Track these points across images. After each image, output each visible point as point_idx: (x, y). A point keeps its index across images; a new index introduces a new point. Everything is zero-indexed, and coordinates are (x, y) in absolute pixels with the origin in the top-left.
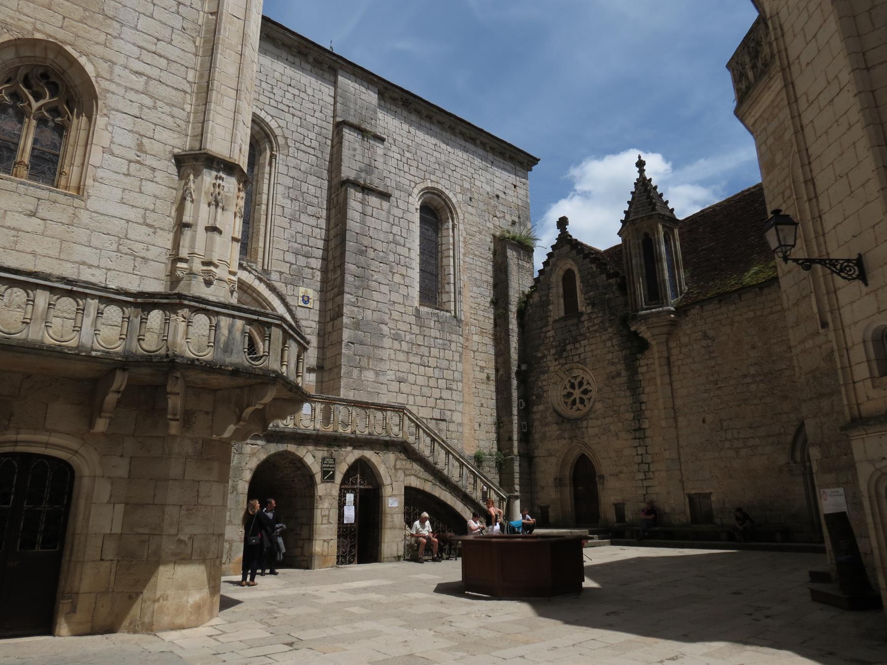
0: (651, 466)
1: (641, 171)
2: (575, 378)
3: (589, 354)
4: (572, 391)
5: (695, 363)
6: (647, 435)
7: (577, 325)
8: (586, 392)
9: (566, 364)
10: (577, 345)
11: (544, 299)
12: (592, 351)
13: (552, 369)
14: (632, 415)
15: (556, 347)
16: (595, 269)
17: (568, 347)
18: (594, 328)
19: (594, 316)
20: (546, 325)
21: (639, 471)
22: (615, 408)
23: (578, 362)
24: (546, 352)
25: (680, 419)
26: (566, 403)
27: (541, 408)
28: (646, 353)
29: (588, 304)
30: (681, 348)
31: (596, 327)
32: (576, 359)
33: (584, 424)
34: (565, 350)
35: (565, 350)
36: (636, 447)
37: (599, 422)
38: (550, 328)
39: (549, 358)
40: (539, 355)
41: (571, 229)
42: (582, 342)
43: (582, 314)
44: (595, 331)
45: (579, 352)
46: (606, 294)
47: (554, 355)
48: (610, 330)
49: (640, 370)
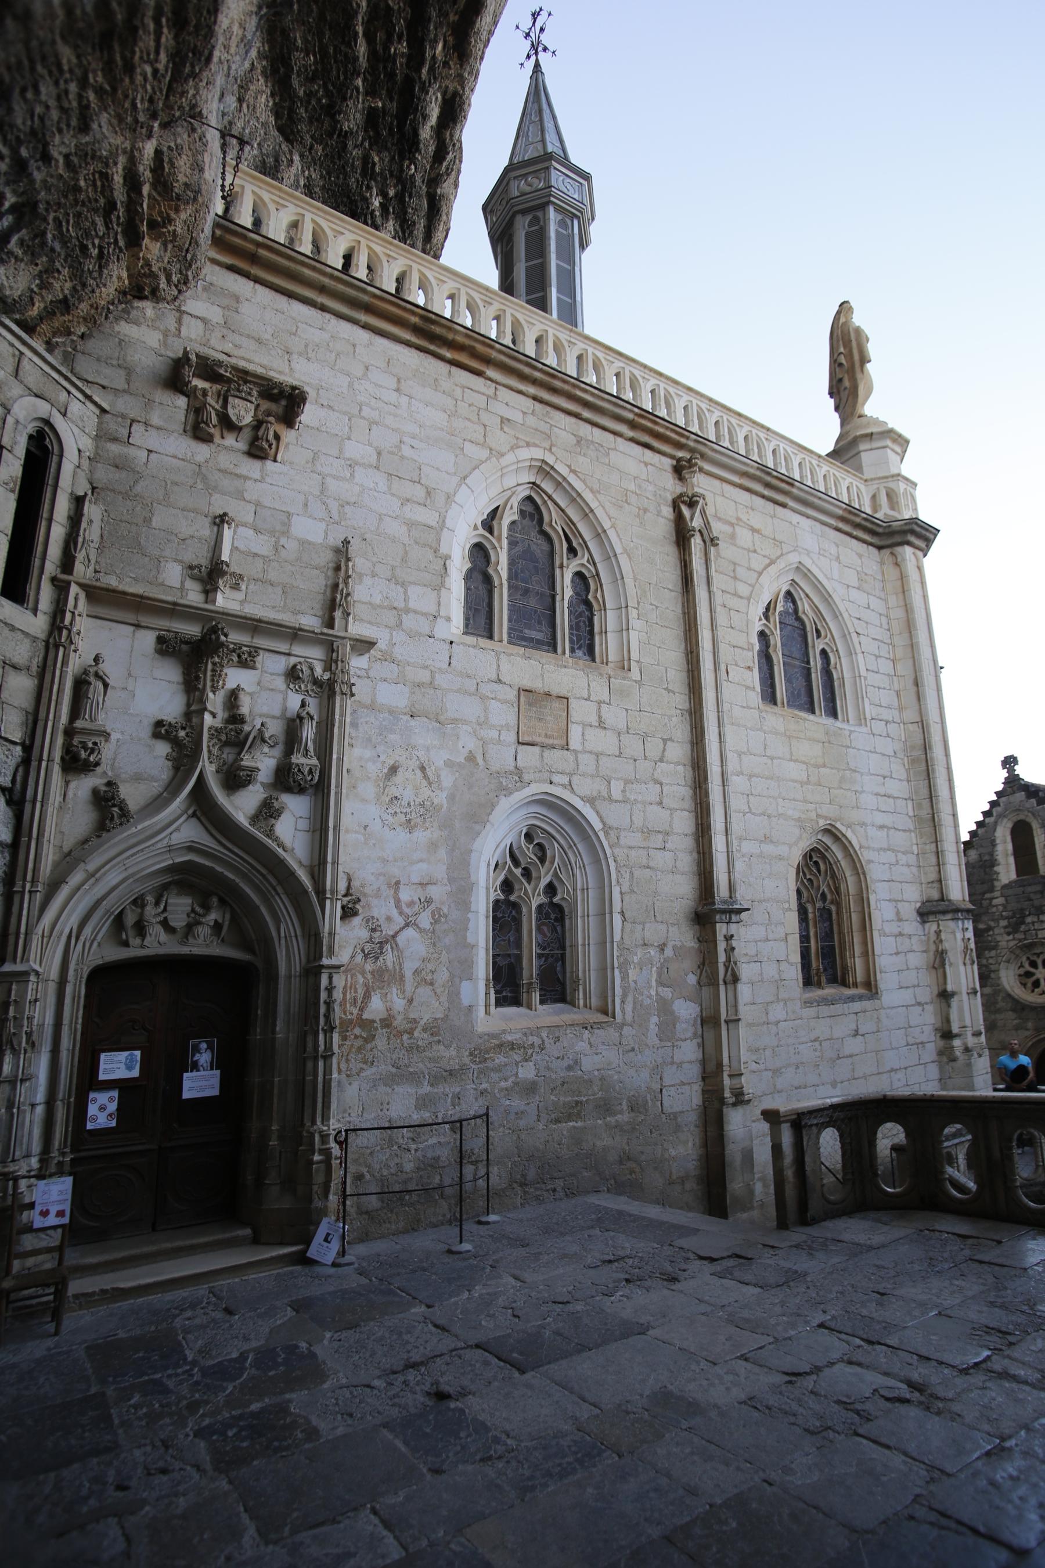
2: (1038, 955)
4: (1032, 970)
9: (1025, 939)
11: (987, 858)
13: (1003, 944)
15: (1007, 918)
17: (1029, 920)
26: (1024, 985)
34: (1023, 923)
35: (1023, 923)
38: (997, 894)
47: (1005, 927)
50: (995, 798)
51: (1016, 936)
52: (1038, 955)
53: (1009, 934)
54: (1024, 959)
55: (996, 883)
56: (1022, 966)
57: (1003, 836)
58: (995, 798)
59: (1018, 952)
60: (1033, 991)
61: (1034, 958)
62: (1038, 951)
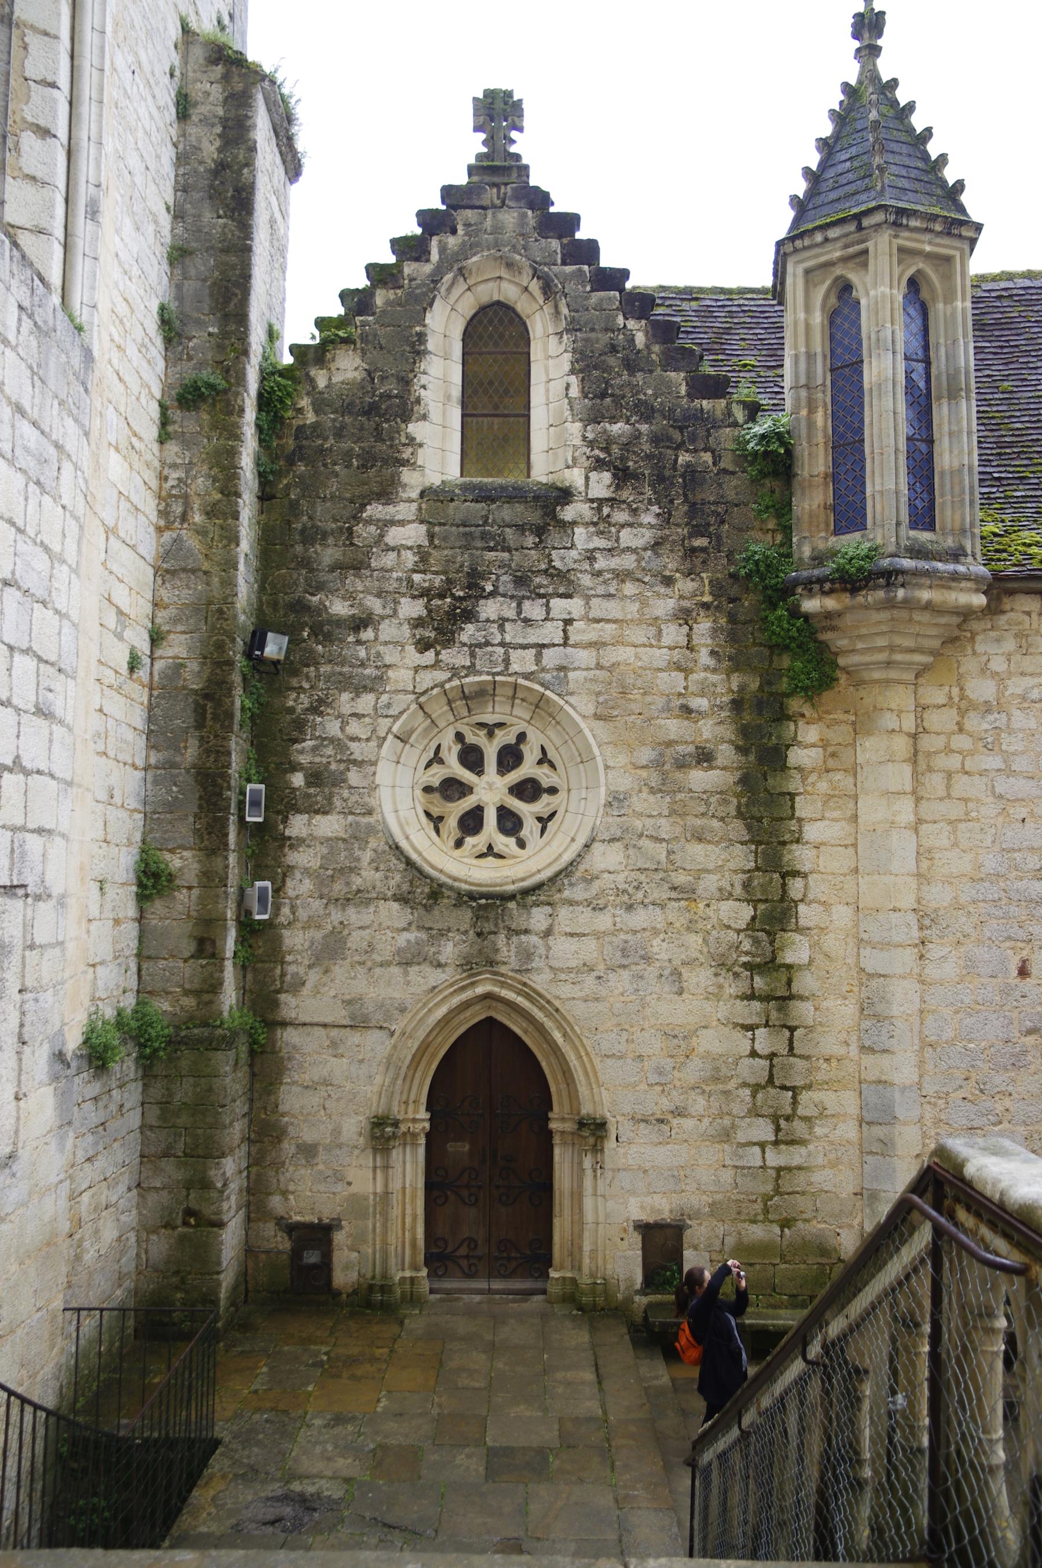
0: (804, 1097)
1: (869, 52)
2: (490, 730)
3: (584, 657)
4: (466, 775)
5: (1008, 772)
6: (795, 989)
7: (540, 531)
8: (528, 790)
9: (471, 669)
10: (533, 609)
12: (597, 645)
13: (400, 677)
14: (746, 912)
15: (425, 593)
16: (640, 339)
18: (615, 563)
19: (621, 516)
20: (387, 493)
21: (755, 1112)
22: (681, 879)
23: (527, 676)
24: (375, 605)
25: (935, 951)
26: (437, 821)
27: (329, 825)
28: (827, 696)
29: (599, 465)
30: (962, 713)
31: (628, 562)
32: (522, 661)
33: (538, 918)
36: (750, 1028)
37: (604, 921)
38: (405, 510)
39: (388, 630)
40: (339, 608)
41: (524, 145)
42: (556, 603)
43: (565, 495)
44: (622, 576)
45: (534, 636)
46: (679, 447)
47: (418, 623)
48: (686, 585)
49: (796, 756)
50: (437, 204)
51: (445, 655)
52: (490, 730)
53: (423, 646)
54: (447, 739)
55: (407, 475)
56: (437, 759)
57: (444, 326)
58: (437, 204)
59: (439, 710)
60: (459, 844)
61: (478, 738)
62: (490, 719)
